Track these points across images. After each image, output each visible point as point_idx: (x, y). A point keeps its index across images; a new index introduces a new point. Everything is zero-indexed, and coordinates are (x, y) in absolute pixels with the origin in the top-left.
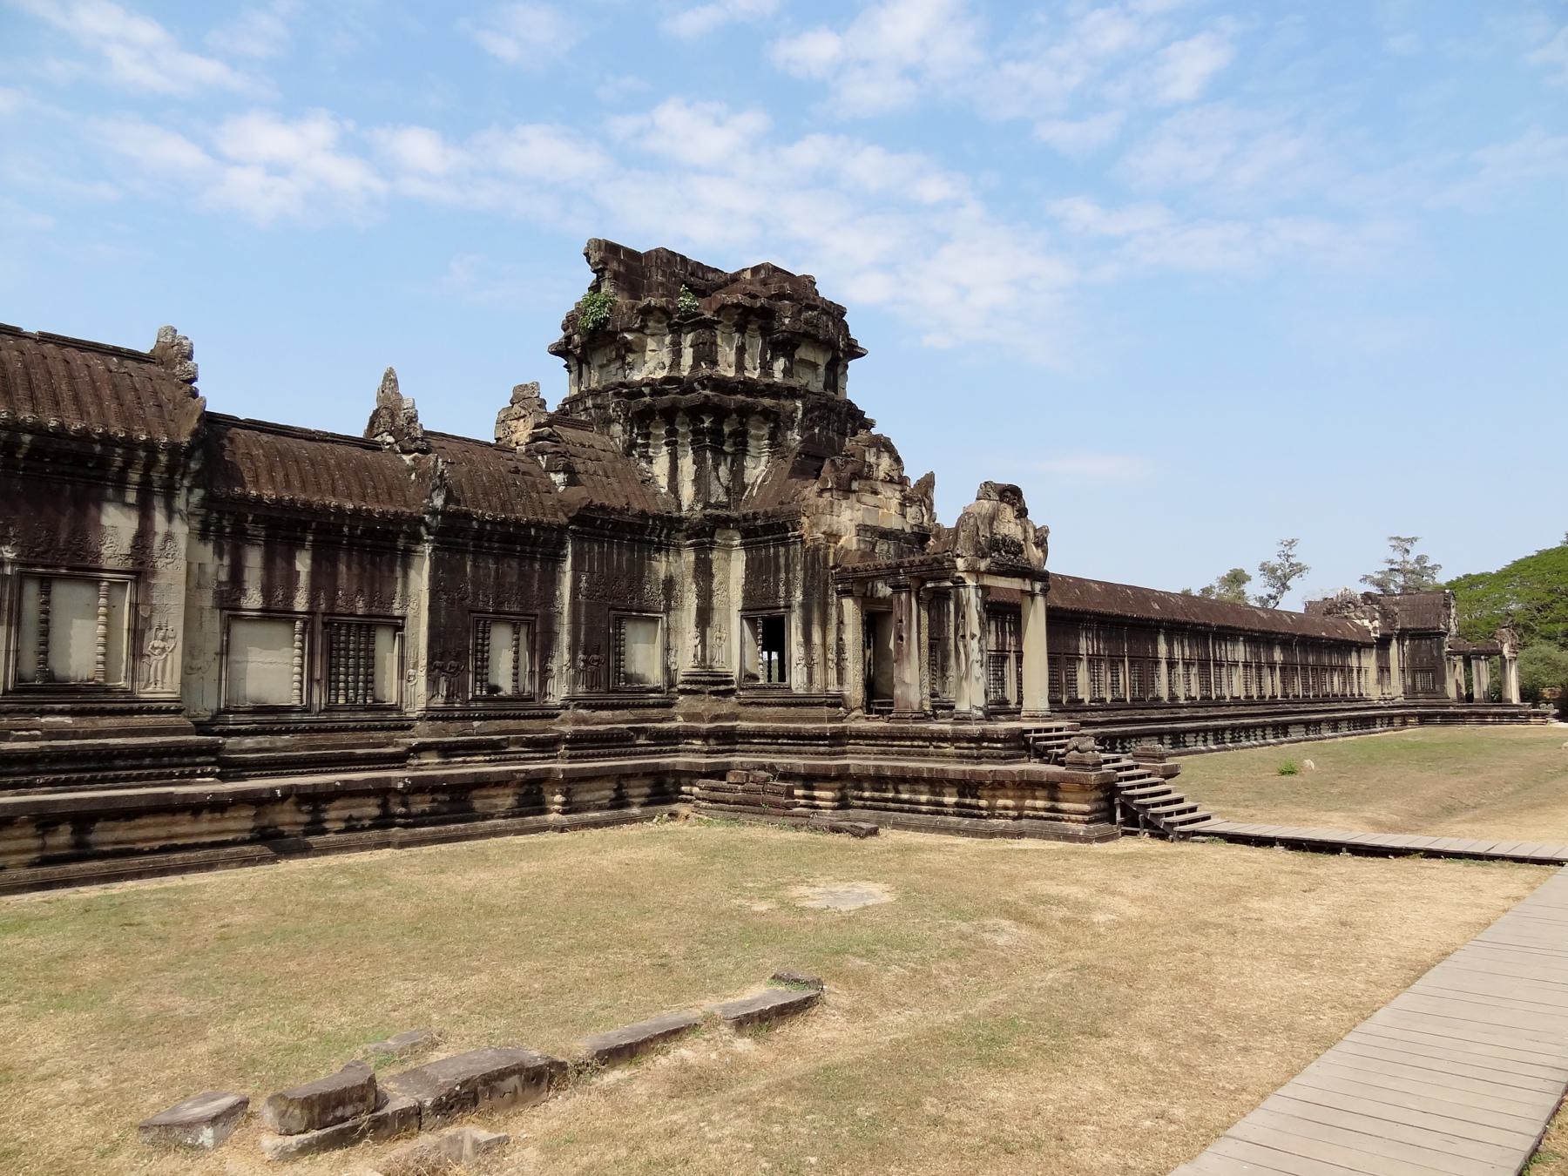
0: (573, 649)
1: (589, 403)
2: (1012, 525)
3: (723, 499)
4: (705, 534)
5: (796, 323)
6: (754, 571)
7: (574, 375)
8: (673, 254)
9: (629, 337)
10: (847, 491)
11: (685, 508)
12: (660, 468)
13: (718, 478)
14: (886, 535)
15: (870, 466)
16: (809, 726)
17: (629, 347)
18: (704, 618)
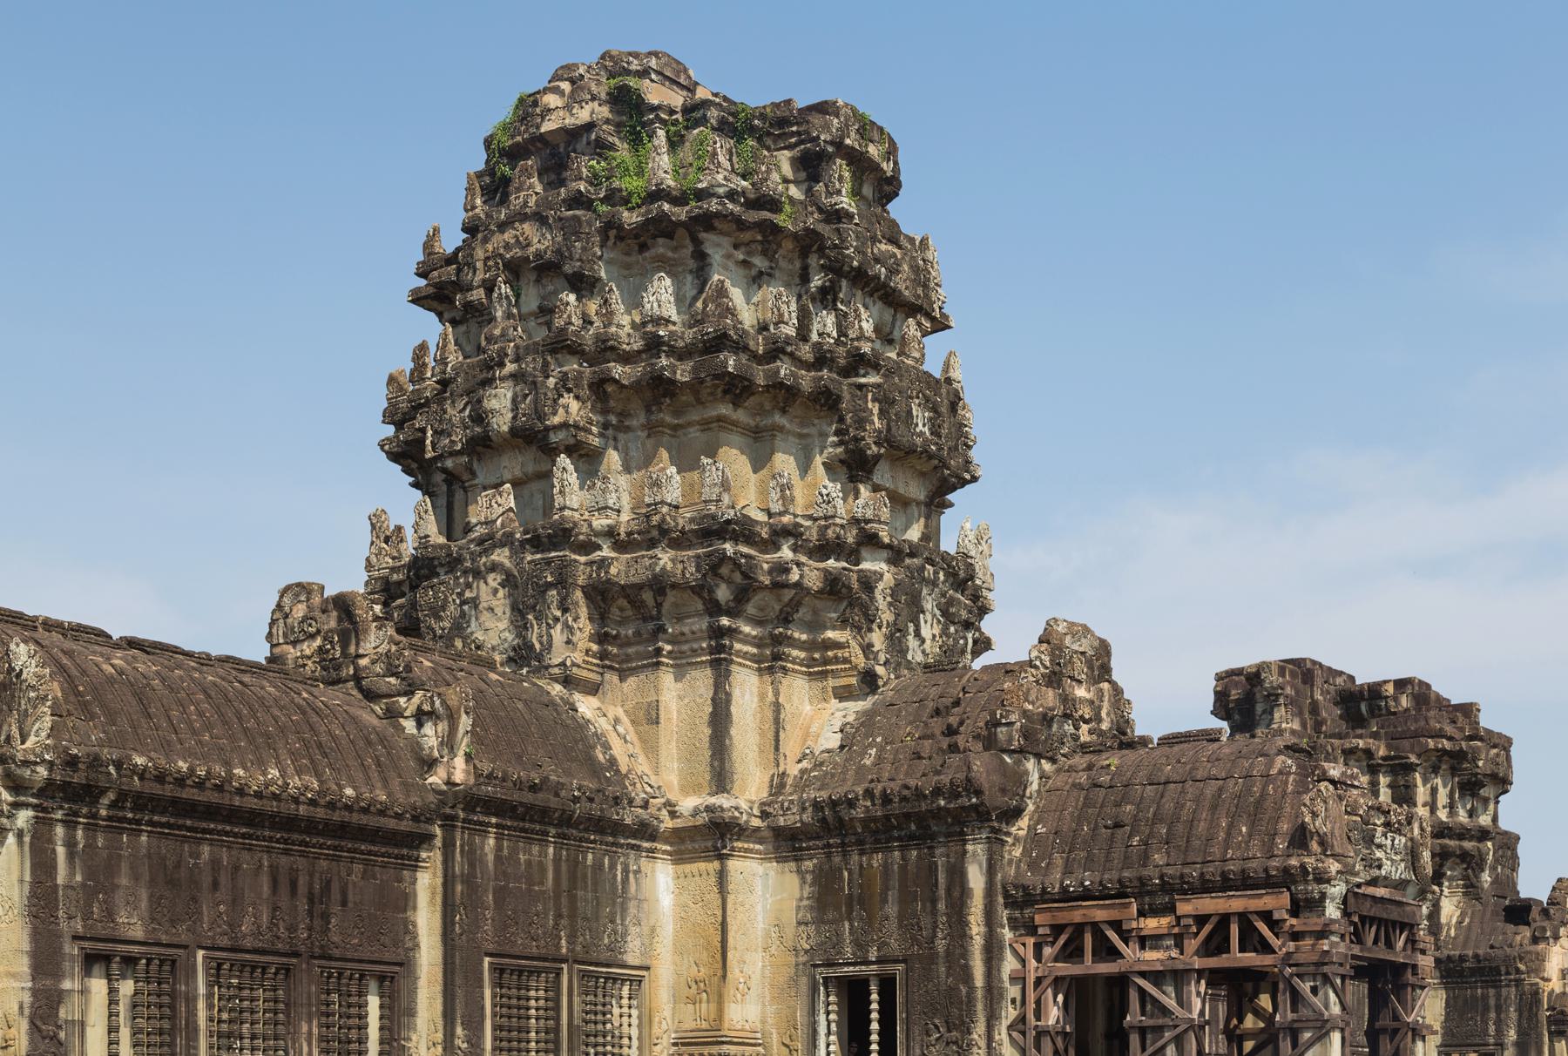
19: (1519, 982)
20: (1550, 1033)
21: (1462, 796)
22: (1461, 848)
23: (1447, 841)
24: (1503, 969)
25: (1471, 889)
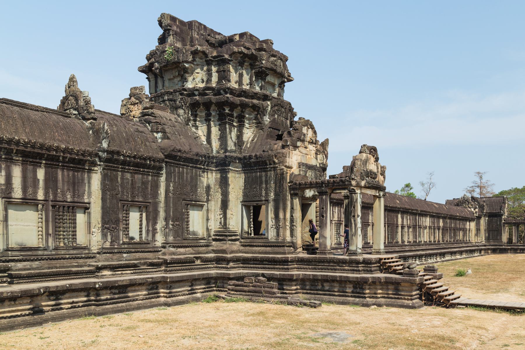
0: (166, 219)
1: (166, 98)
2: (373, 165)
3: (233, 148)
5: (263, 62)
7: (153, 82)
8: (200, 24)
9: (187, 65)
10: (296, 147)
11: (214, 152)
12: (201, 132)
13: (231, 138)
14: (310, 167)
15: (304, 135)
16: (279, 256)
17: (186, 70)
19: (275, 169)
20: (291, 195)
21: (257, 80)
22: (252, 102)
23: (243, 99)
24: (268, 162)
25: (259, 125)
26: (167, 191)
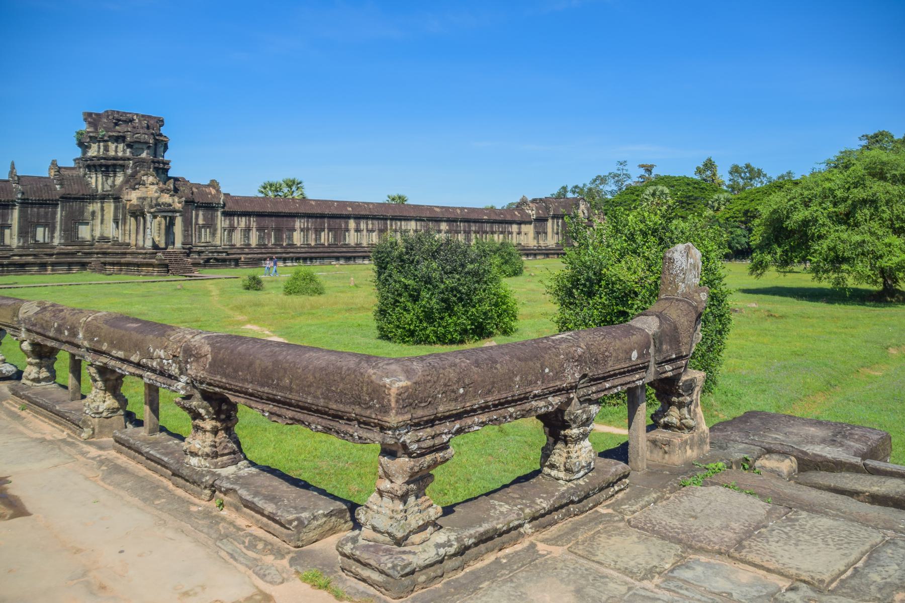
0: (61, 231)
4: (103, 198)
6: (116, 209)
12: (93, 181)
18: (102, 222)
26: (61, 216)
